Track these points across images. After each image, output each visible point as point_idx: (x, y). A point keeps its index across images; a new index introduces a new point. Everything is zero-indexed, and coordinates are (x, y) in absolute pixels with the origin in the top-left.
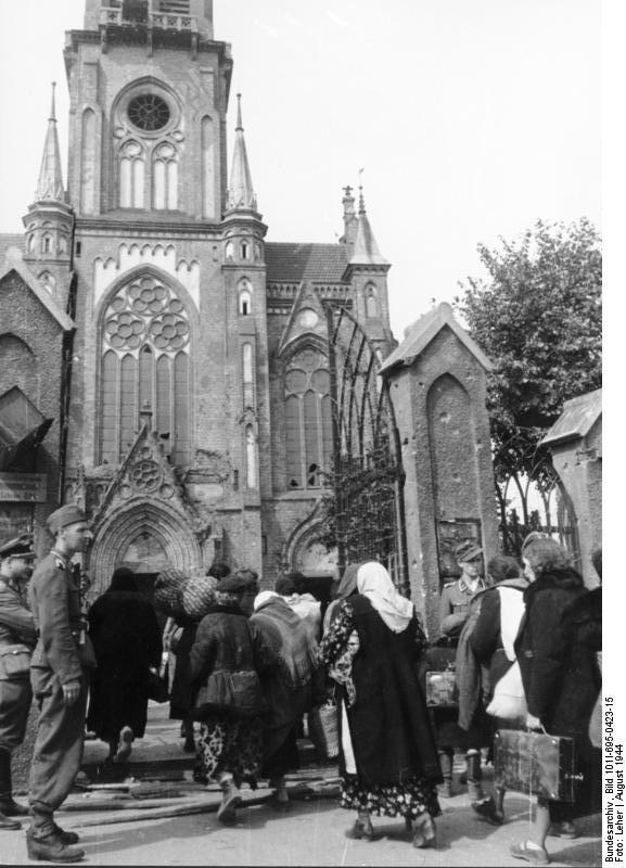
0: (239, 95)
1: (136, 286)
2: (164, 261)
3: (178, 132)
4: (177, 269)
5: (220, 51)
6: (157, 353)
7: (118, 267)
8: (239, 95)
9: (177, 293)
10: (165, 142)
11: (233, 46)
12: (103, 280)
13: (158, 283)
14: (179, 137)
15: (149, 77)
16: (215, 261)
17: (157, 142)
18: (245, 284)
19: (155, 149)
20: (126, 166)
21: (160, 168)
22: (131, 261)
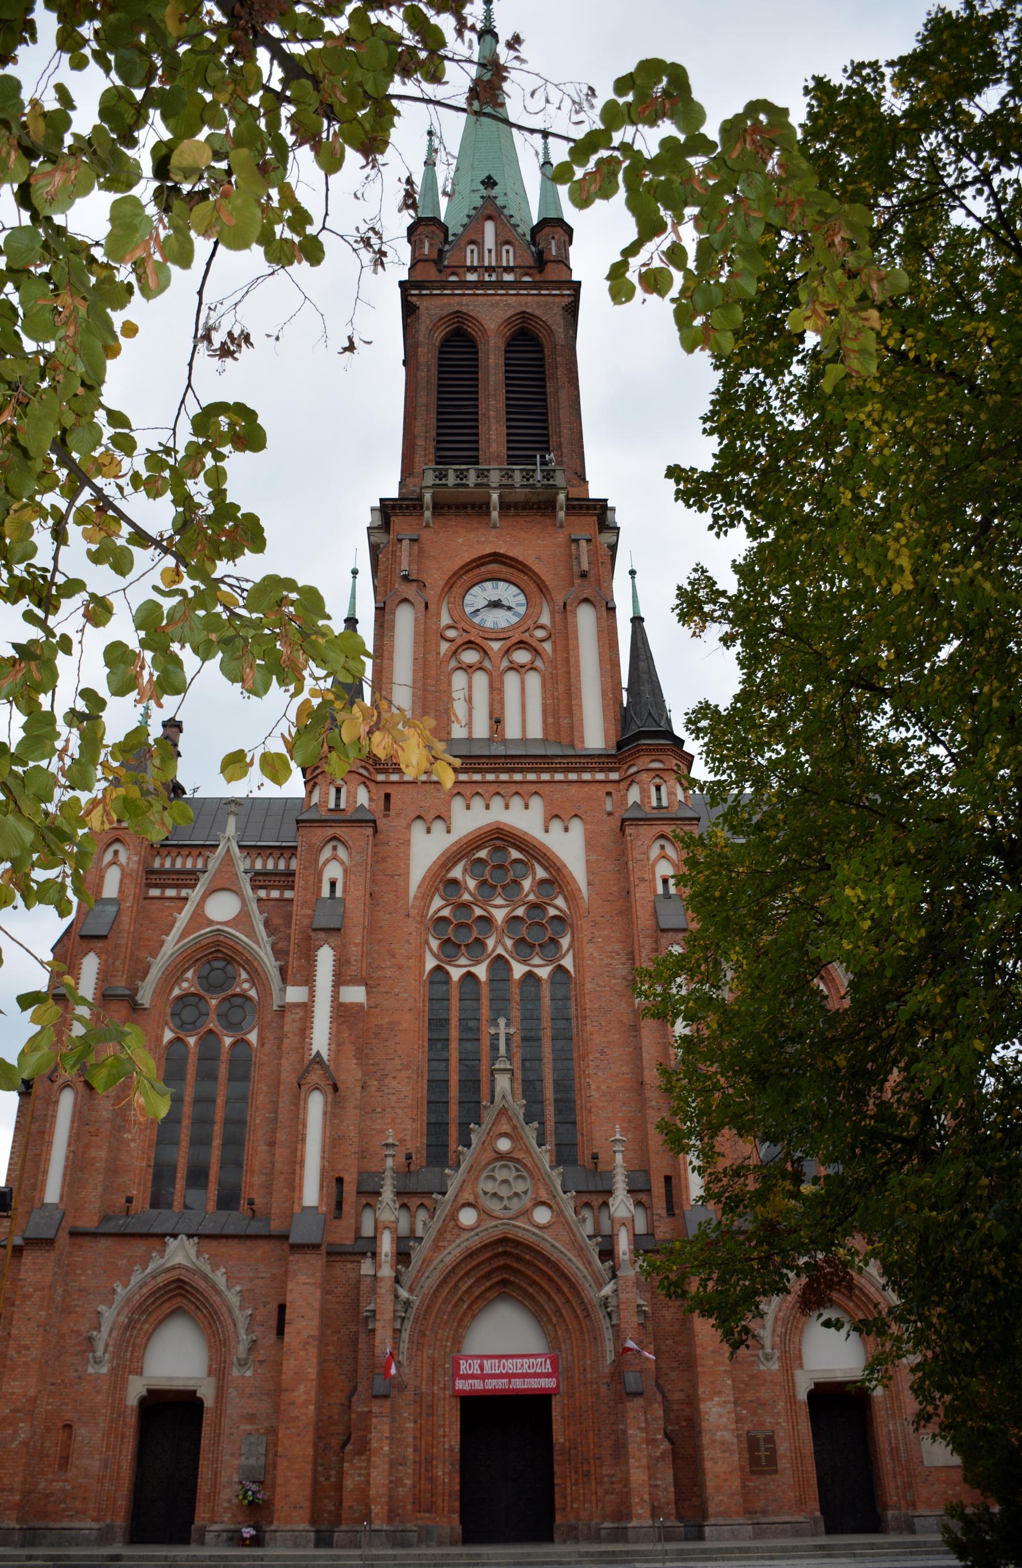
0: (632, 573)
1: (480, 860)
2: (525, 818)
3: (542, 627)
4: (547, 831)
5: (601, 510)
6: (519, 970)
7: (449, 832)
8: (632, 573)
9: (546, 869)
10: (521, 642)
11: (684, 353)
12: (425, 849)
13: (515, 854)
14: (540, 634)
15: (495, 554)
16: (610, 814)
17: (509, 643)
18: (662, 847)
19: (508, 651)
20: (459, 680)
21: (511, 680)
22: (469, 819)
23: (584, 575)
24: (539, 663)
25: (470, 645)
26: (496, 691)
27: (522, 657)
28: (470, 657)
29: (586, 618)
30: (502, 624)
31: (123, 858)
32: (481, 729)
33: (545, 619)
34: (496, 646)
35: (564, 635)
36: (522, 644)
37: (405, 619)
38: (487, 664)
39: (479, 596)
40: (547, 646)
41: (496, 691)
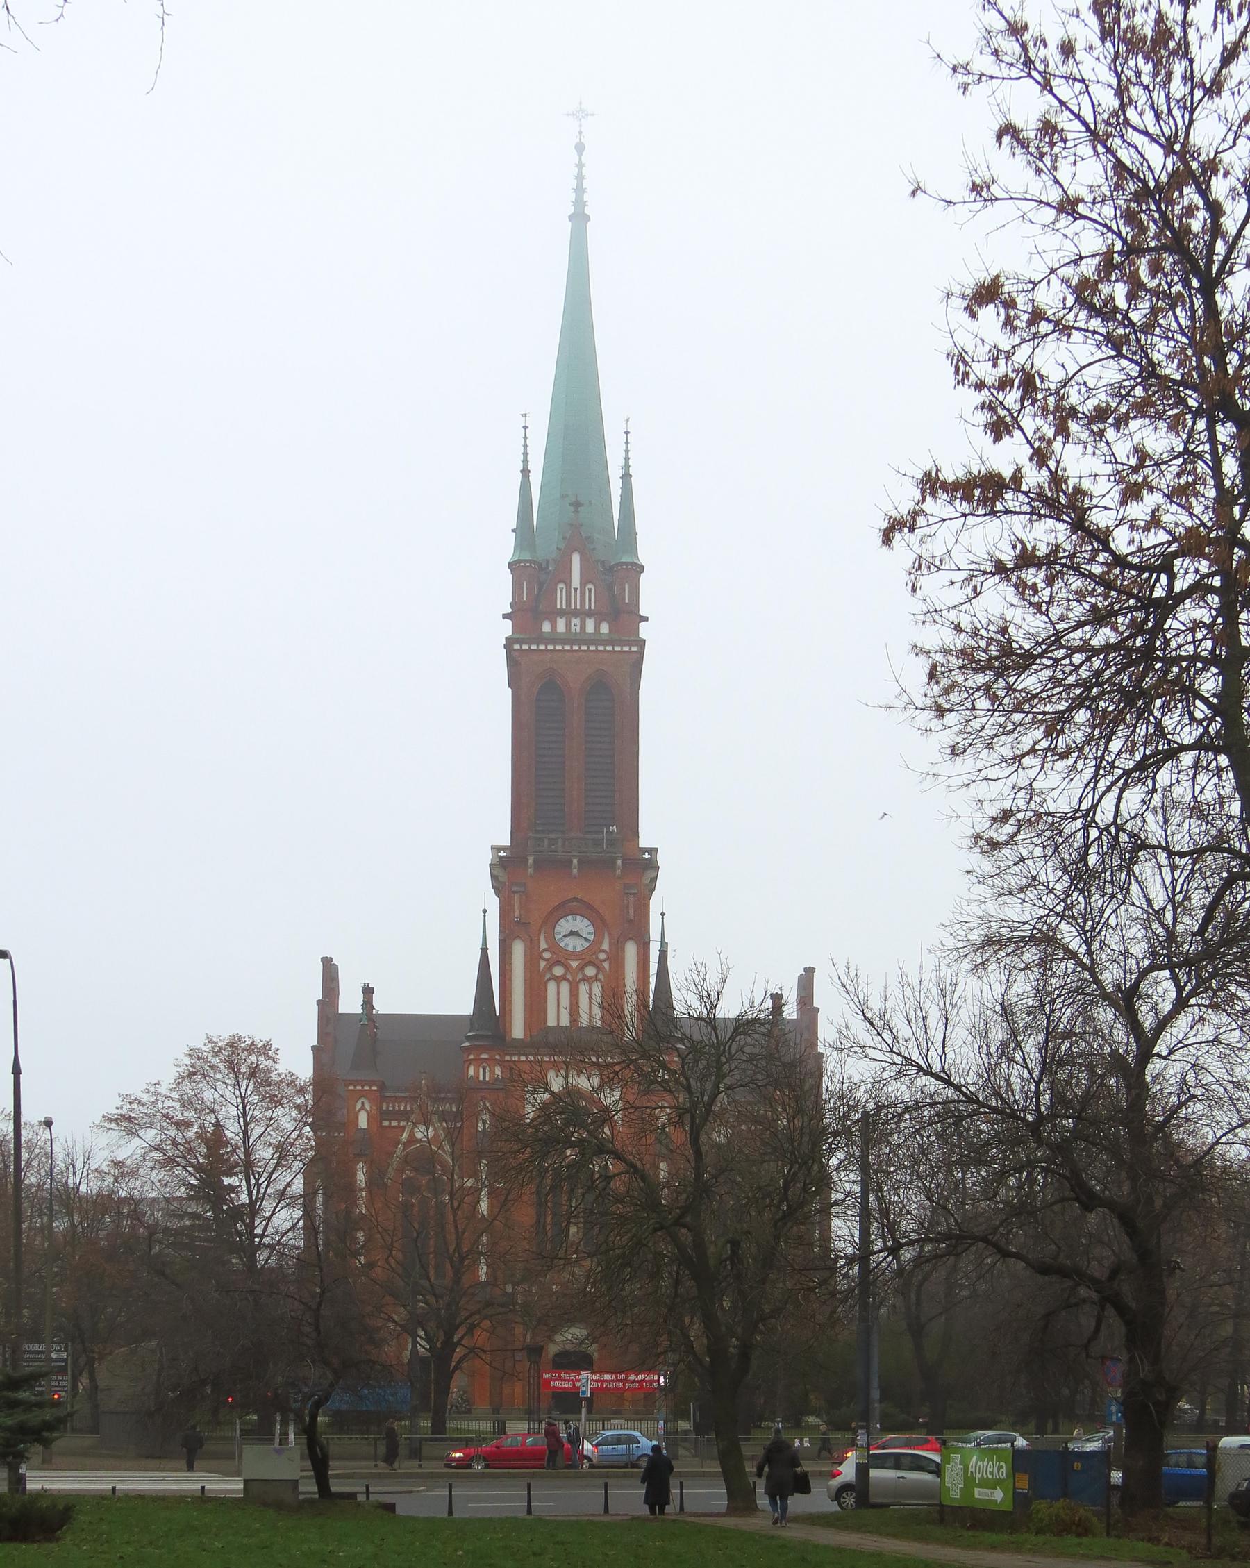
0: (663, 914)
8: (663, 914)
20: (552, 987)
23: (630, 921)
24: (601, 976)
25: (558, 963)
26: (574, 995)
27: (590, 971)
28: (558, 971)
29: (631, 950)
30: (579, 948)
31: (367, 1106)
32: (565, 1021)
33: (606, 946)
34: (574, 964)
35: (617, 959)
36: (590, 963)
37: (518, 950)
38: (569, 976)
39: (565, 925)
40: (606, 965)
41: (574, 995)
